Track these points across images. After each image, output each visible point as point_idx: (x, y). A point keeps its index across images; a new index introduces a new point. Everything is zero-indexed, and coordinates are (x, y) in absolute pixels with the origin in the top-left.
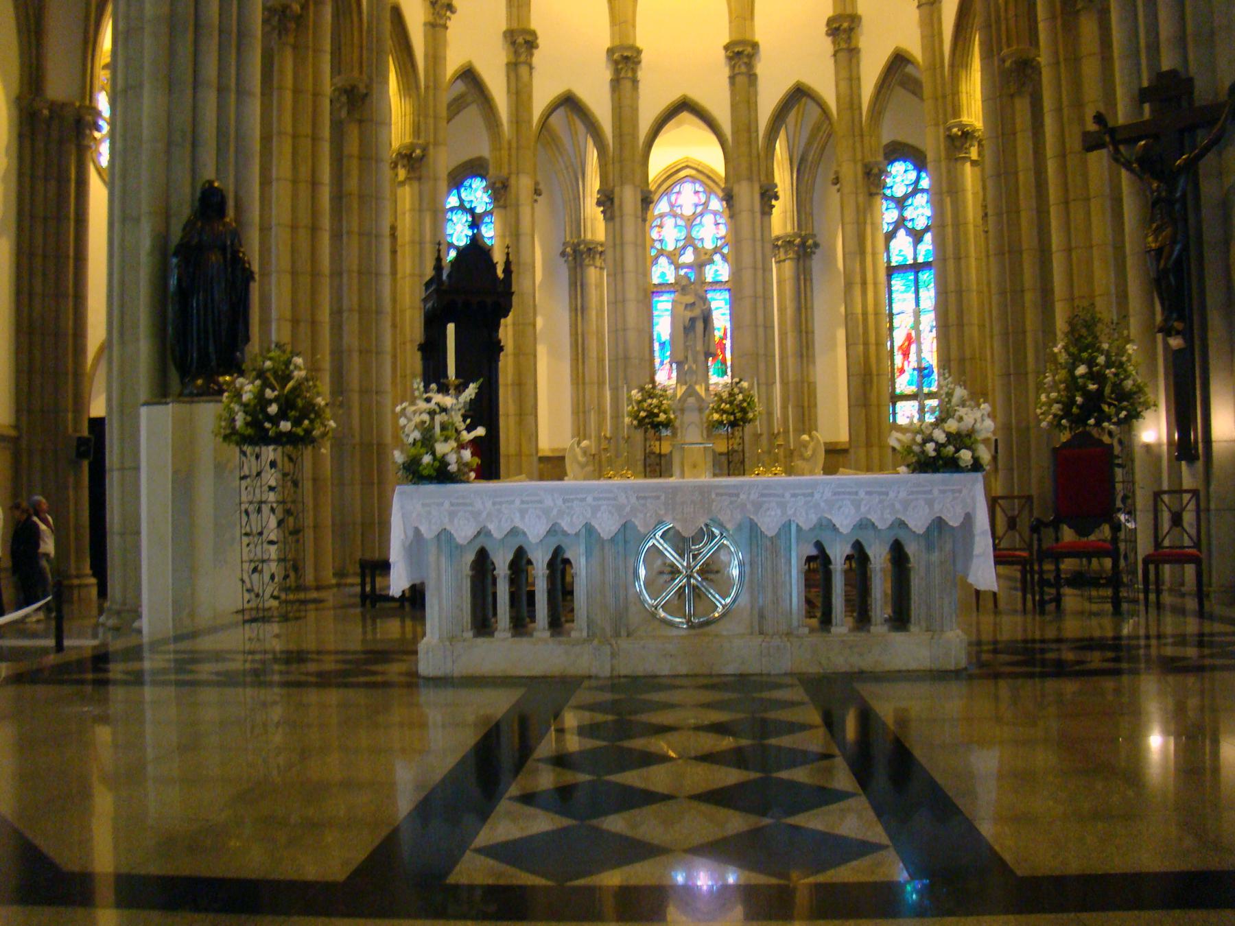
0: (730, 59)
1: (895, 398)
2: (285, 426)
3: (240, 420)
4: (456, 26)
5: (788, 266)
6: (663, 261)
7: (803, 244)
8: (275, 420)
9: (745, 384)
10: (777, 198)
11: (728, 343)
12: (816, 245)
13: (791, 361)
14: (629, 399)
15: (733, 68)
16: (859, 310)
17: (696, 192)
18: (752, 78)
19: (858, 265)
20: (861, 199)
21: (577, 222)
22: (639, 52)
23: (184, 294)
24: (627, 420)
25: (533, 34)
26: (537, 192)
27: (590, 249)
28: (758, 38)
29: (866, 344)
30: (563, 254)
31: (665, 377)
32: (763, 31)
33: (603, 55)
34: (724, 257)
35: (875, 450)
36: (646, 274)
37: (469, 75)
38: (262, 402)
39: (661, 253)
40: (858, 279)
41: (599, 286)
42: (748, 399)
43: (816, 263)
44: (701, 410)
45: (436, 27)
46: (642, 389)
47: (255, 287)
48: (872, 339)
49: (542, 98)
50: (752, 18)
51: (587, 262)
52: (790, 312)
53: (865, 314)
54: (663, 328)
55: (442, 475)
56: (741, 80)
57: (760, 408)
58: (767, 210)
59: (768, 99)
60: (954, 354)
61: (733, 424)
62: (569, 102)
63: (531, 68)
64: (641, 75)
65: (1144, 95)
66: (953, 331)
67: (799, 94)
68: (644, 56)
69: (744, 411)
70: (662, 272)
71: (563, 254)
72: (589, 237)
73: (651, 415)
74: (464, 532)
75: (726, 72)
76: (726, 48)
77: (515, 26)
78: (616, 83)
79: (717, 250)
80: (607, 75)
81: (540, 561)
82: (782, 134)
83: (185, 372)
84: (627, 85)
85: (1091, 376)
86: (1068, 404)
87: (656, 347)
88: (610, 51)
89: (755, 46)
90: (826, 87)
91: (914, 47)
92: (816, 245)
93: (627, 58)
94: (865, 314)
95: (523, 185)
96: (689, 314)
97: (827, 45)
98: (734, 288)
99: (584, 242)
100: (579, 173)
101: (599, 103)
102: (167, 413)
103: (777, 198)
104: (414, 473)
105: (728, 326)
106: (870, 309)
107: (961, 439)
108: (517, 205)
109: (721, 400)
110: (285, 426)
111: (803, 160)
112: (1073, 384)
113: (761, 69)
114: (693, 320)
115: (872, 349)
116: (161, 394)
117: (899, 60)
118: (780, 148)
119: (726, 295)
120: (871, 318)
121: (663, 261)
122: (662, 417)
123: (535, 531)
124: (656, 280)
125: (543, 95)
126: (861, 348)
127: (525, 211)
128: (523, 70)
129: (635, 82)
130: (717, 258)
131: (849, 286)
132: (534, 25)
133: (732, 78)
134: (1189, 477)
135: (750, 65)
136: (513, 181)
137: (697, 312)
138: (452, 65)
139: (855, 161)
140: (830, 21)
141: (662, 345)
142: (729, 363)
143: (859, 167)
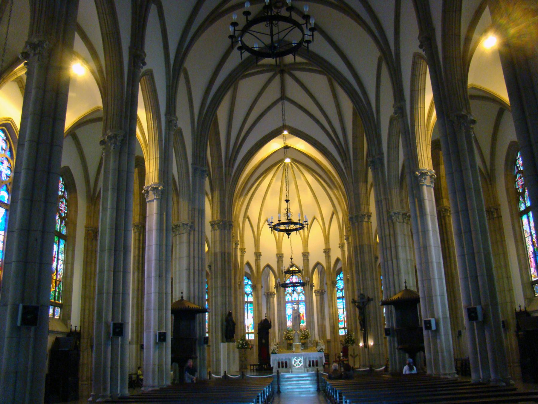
0: (303, 256)
1: (344, 328)
2: (246, 346)
3: (240, 346)
4: (246, 255)
5: (318, 297)
6: (288, 295)
7: (322, 291)
8: (245, 346)
9: (307, 331)
10: (314, 286)
11: (305, 315)
12: (325, 292)
13: (320, 320)
14: (284, 334)
15: (304, 258)
16: (332, 312)
17: (296, 278)
18: (308, 260)
19: (331, 303)
20: (332, 288)
21: (268, 287)
22: (283, 254)
23: (227, 327)
24: (283, 338)
25: (260, 253)
26: (262, 287)
27: (271, 294)
28: (309, 251)
29: (333, 320)
30: (264, 295)
31: (289, 324)
32: (311, 249)
33: (275, 255)
34: (303, 294)
35: (336, 343)
36: (285, 298)
37: (248, 264)
38: (243, 343)
39: (288, 293)
40: (331, 306)
41: (273, 302)
42: (308, 333)
43: (325, 296)
44: (298, 336)
45: (242, 256)
46: (286, 332)
47: (236, 326)
48: (335, 319)
49: (262, 266)
50: (308, 247)
51: (270, 296)
52: (319, 307)
53: (333, 313)
54: (289, 311)
55: (275, 353)
56: (306, 261)
57: (310, 336)
58: (312, 289)
59: (311, 266)
60: (349, 323)
61: (305, 339)
62: (268, 266)
63: (260, 260)
64: (284, 259)
65: (358, 297)
66: (349, 319)
67: (318, 264)
68: (284, 255)
69: (307, 336)
70: (288, 298)
71: (264, 295)
72: (271, 291)
73: (288, 337)
74: (277, 358)
75: (302, 258)
76: (302, 253)
77: (257, 252)
78: (278, 262)
79: (301, 292)
80: (276, 260)
81: (284, 362)
82: (316, 268)
83: (226, 337)
84: (280, 262)
85: (348, 338)
86: (345, 341)
87: (287, 316)
88: (277, 255)
89: (308, 253)
90: (324, 263)
91: (340, 258)
92: (325, 292)
93: (280, 256)
94: (333, 313)
95: (259, 286)
96: (295, 315)
97: (324, 254)
98: (305, 301)
99: (270, 292)
100: (268, 276)
101: (275, 266)
102: (226, 344)
103: (314, 286)
104: (273, 353)
105: (305, 311)
106: (334, 312)
107: (322, 349)
108: (258, 291)
109: (302, 334)
110: (246, 346)
111: (321, 272)
112: (346, 339)
113: (310, 258)
114: (296, 316)
115: (335, 321)
116: (223, 341)
117: (338, 260)
118: (316, 270)
119: (304, 303)
120: (334, 314)
121: (288, 295)
122: (291, 338)
123: (284, 358)
124: (287, 300)
125: (262, 265)
126: (332, 321)
127: (260, 292)
128: (258, 261)
129: (282, 261)
130: (301, 294)
131: (329, 307)
132: (260, 251)
133: (304, 260)
134: (366, 350)
135: (307, 257)
136: (257, 285)
137: (297, 315)
138: (245, 262)
139: (330, 280)
140: (324, 250)
141: (288, 316)
142: (305, 320)
143: (331, 282)
